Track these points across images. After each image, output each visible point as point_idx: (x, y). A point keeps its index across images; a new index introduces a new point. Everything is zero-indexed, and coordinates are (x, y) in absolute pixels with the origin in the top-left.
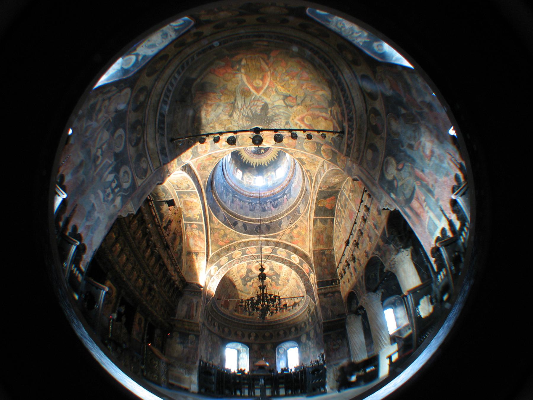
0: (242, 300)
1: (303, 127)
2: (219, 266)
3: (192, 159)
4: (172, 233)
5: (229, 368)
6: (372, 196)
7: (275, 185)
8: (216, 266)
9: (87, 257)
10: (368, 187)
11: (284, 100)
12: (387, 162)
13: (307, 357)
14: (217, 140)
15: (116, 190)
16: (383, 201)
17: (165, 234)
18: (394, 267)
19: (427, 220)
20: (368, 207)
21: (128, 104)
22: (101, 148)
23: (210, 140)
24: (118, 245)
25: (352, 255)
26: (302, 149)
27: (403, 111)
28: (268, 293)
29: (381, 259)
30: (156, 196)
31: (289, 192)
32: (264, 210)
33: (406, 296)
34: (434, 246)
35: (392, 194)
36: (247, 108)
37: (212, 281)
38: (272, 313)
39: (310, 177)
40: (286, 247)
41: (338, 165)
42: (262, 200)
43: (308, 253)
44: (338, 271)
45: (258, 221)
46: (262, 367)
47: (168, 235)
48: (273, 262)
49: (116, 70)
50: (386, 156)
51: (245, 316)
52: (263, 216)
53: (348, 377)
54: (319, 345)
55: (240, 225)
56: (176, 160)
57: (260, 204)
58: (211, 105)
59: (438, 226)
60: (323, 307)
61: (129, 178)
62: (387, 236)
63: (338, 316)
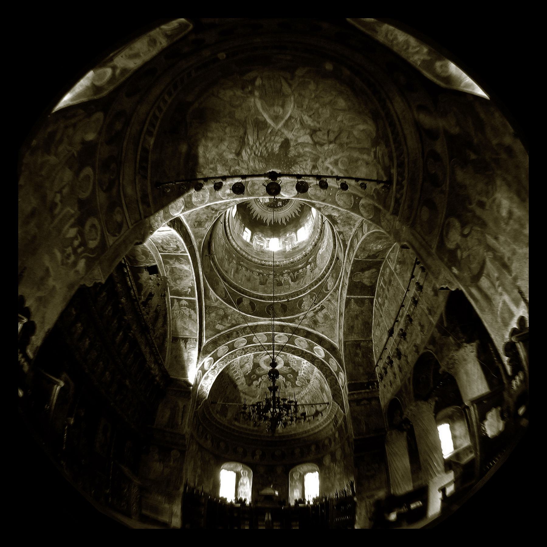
0: (245, 405)
1: (336, 173)
2: (216, 358)
3: (183, 211)
4: (152, 311)
5: (224, 497)
6: (427, 271)
8: (212, 358)
9: (38, 339)
10: (421, 257)
11: (311, 136)
12: (449, 224)
13: (330, 485)
14: (218, 187)
15: (79, 250)
16: (441, 277)
17: (143, 312)
18: (453, 367)
19: (501, 305)
20: (421, 284)
21: (100, 133)
22: (60, 192)
23: (208, 187)
24: (79, 325)
25: (397, 349)
27: (473, 157)
28: (281, 398)
29: (436, 356)
30: (133, 259)
31: (315, 260)
33: (468, 407)
34: (508, 340)
35: (453, 268)
36: (260, 144)
37: (206, 379)
38: (285, 424)
39: (344, 241)
40: (308, 335)
41: (382, 227)
42: (278, 270)
43: (337, 345)
44: (377, 370)
45: (270, 298)
46: (270, 497)
47: (148, 314)
48: (288, 354)
49: (84, 87)
50: (447, 217)
51: (249, 427)
52: (277, 293)
53: (386, 515)
54: (347, 471)
55: (246, 303)
56: (162, 212)
58: (212, 139)
59: (515, 313)
60: (354, 419)
61: (97, 234)
62: (445, 325)
63: (375, 432)
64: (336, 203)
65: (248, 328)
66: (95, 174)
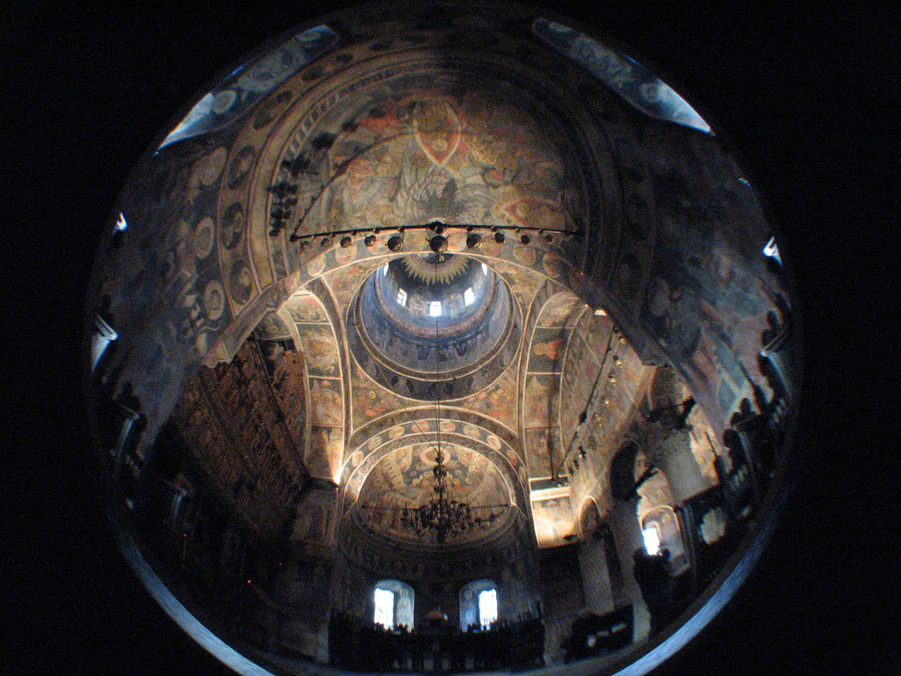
1: (514, 222)
3: (325, 270)
5: (381, 623)
7: (462, 317)
11: (483, 175)
14: (368, 241)
26: (511, 258)
31: (487, 328)
32: (442, 358)
36: (420, 186)
37: (355, 477)
39: (523, 305)
45: (433, 376)
46: (437, 623)
48: (456, 445)
55: (402, 383)
57: (438, 348)
58: (361, 180)
64: (514, 258)
65: (405, 414)
66: (215, 224)
